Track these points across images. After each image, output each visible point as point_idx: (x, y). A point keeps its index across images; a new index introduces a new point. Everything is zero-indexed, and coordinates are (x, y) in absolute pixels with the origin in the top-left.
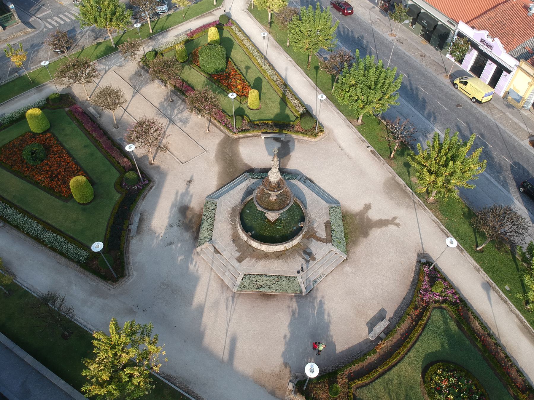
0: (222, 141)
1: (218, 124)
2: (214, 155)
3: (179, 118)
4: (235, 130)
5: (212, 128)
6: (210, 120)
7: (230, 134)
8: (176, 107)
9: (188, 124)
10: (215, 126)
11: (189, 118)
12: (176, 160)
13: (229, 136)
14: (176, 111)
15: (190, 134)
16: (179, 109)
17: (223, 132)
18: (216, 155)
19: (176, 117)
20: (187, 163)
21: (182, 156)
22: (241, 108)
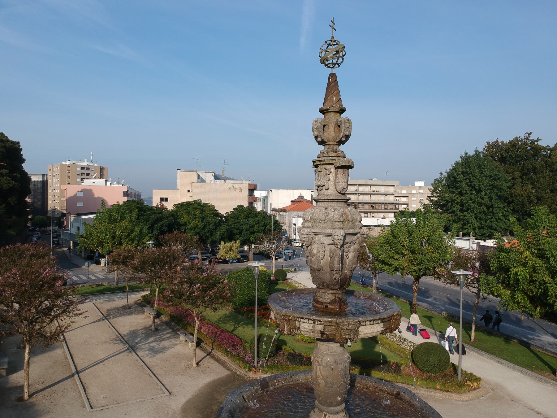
0: (218, 380)
1: (223, 357)
2: (184, 400)
3: (151, 346)
4: (256, 364)
5: (209, 362)
6: (211, 353)
7: (242, 372)
8: (157, 335)
9: (161, 354)
10: (217, 360)
11: (169, 348)
12: (82, 401)
13: (238, 375)
14: (152, 339)
15: (155, 366)
16: (161, 338)
17: (228, 369)
18: (189, 402)
19: (147, 345)
20: (104, 408)
21: (102, 396)
22: (281, 340)
